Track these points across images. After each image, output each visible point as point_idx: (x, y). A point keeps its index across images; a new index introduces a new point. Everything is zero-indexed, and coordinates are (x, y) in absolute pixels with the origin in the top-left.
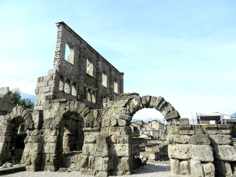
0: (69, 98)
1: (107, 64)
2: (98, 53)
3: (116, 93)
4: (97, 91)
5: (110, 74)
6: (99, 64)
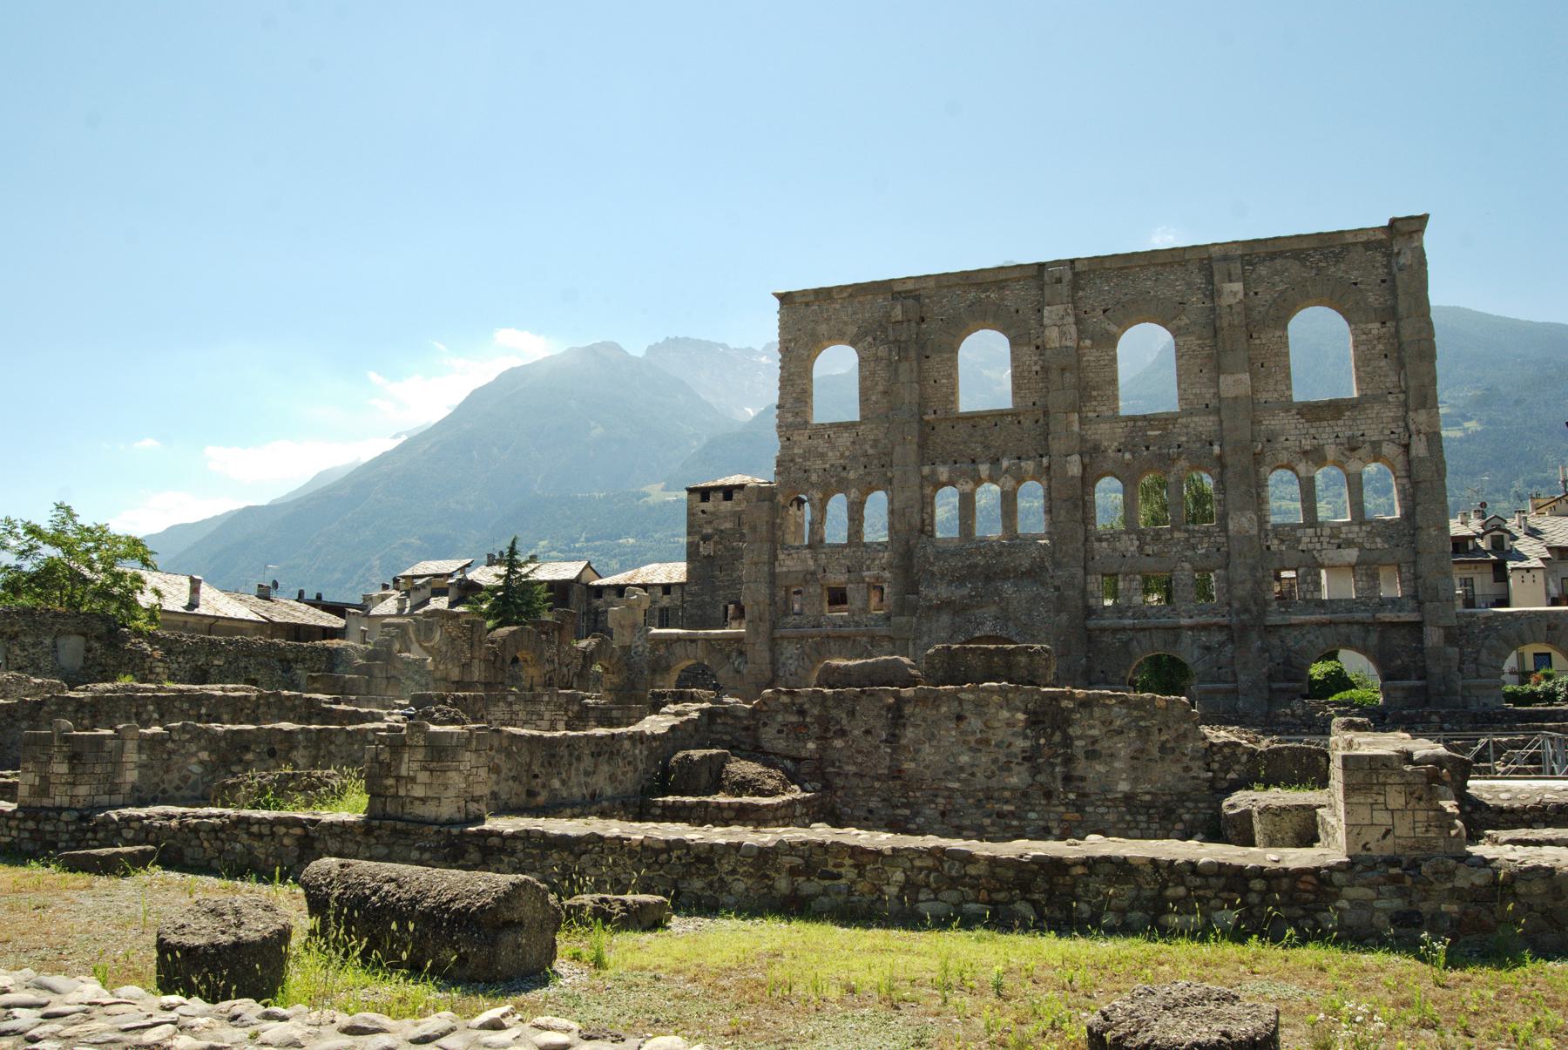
0: (845, 557)
1: (1171, 264)
2: (1041, 267)
3: (1315, 412)
4: (1049, 468)
5: (1213, 310)
6: (1046, 321)
